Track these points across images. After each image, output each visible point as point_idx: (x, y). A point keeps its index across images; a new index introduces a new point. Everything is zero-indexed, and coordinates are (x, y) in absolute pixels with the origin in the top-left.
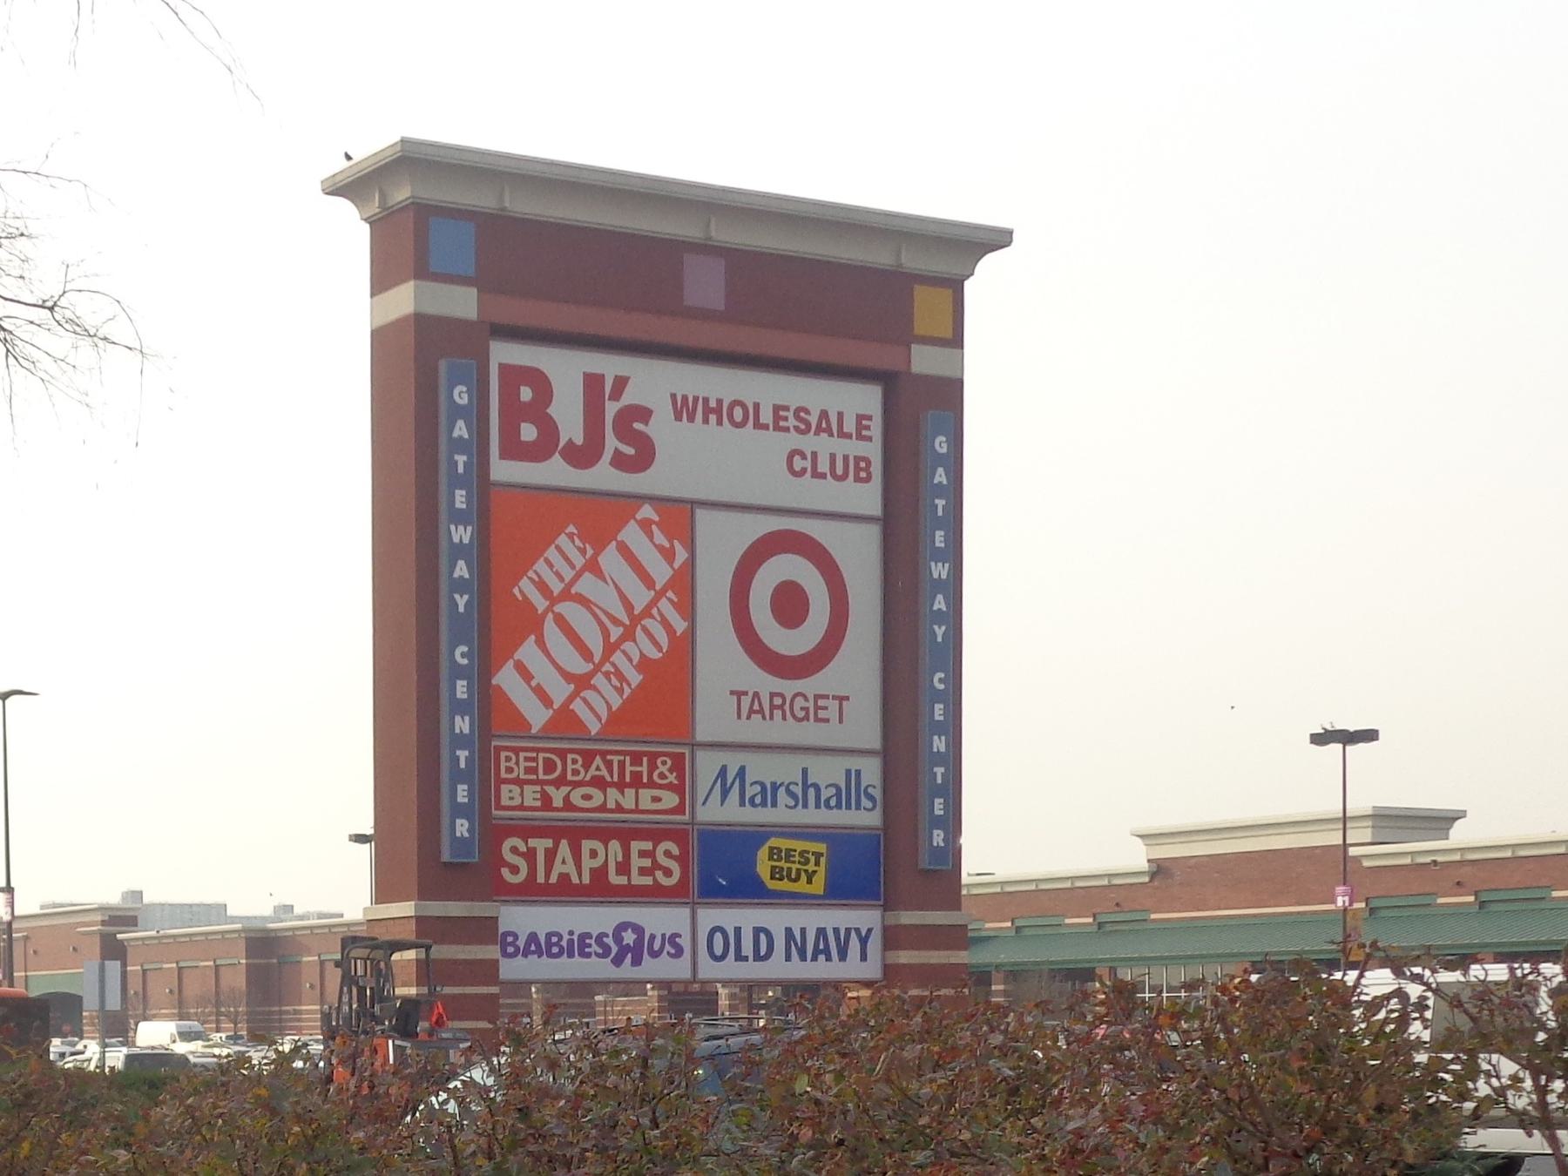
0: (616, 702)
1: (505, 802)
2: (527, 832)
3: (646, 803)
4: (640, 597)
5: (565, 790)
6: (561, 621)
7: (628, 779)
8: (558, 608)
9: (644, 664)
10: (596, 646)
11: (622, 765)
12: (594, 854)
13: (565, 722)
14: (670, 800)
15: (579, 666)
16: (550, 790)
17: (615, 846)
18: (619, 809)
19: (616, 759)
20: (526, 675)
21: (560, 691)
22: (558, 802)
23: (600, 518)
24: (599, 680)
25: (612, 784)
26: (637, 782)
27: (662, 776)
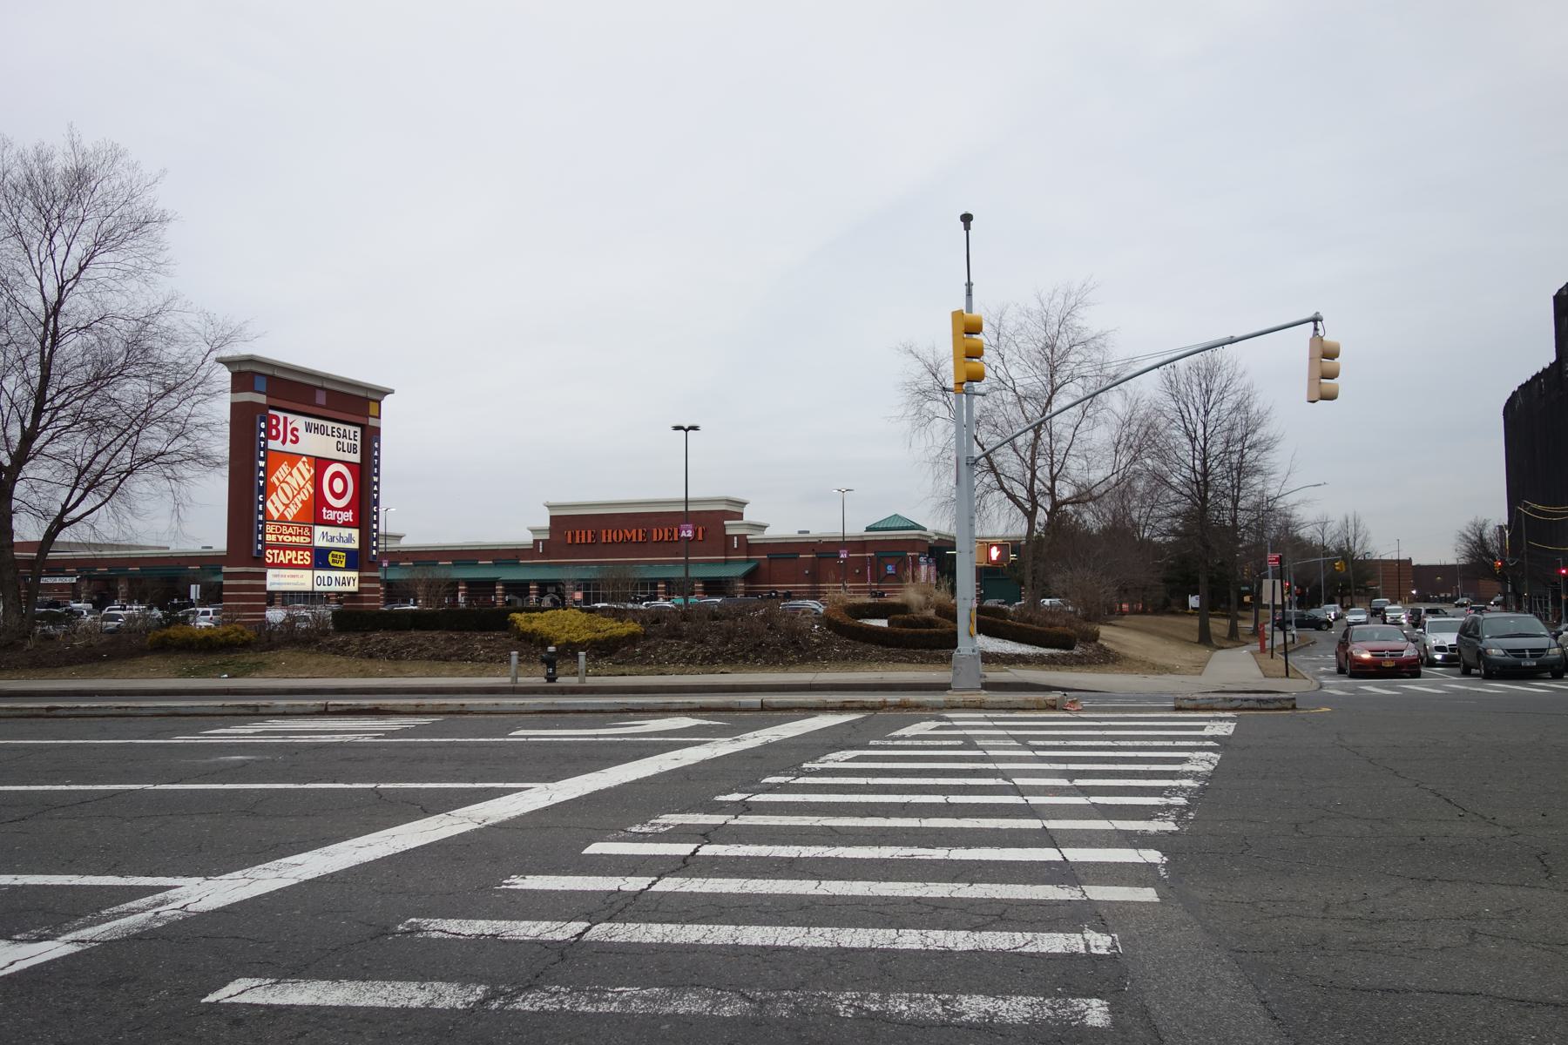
2: (273, 547)
4: (302, 483)
23: (293, 459)
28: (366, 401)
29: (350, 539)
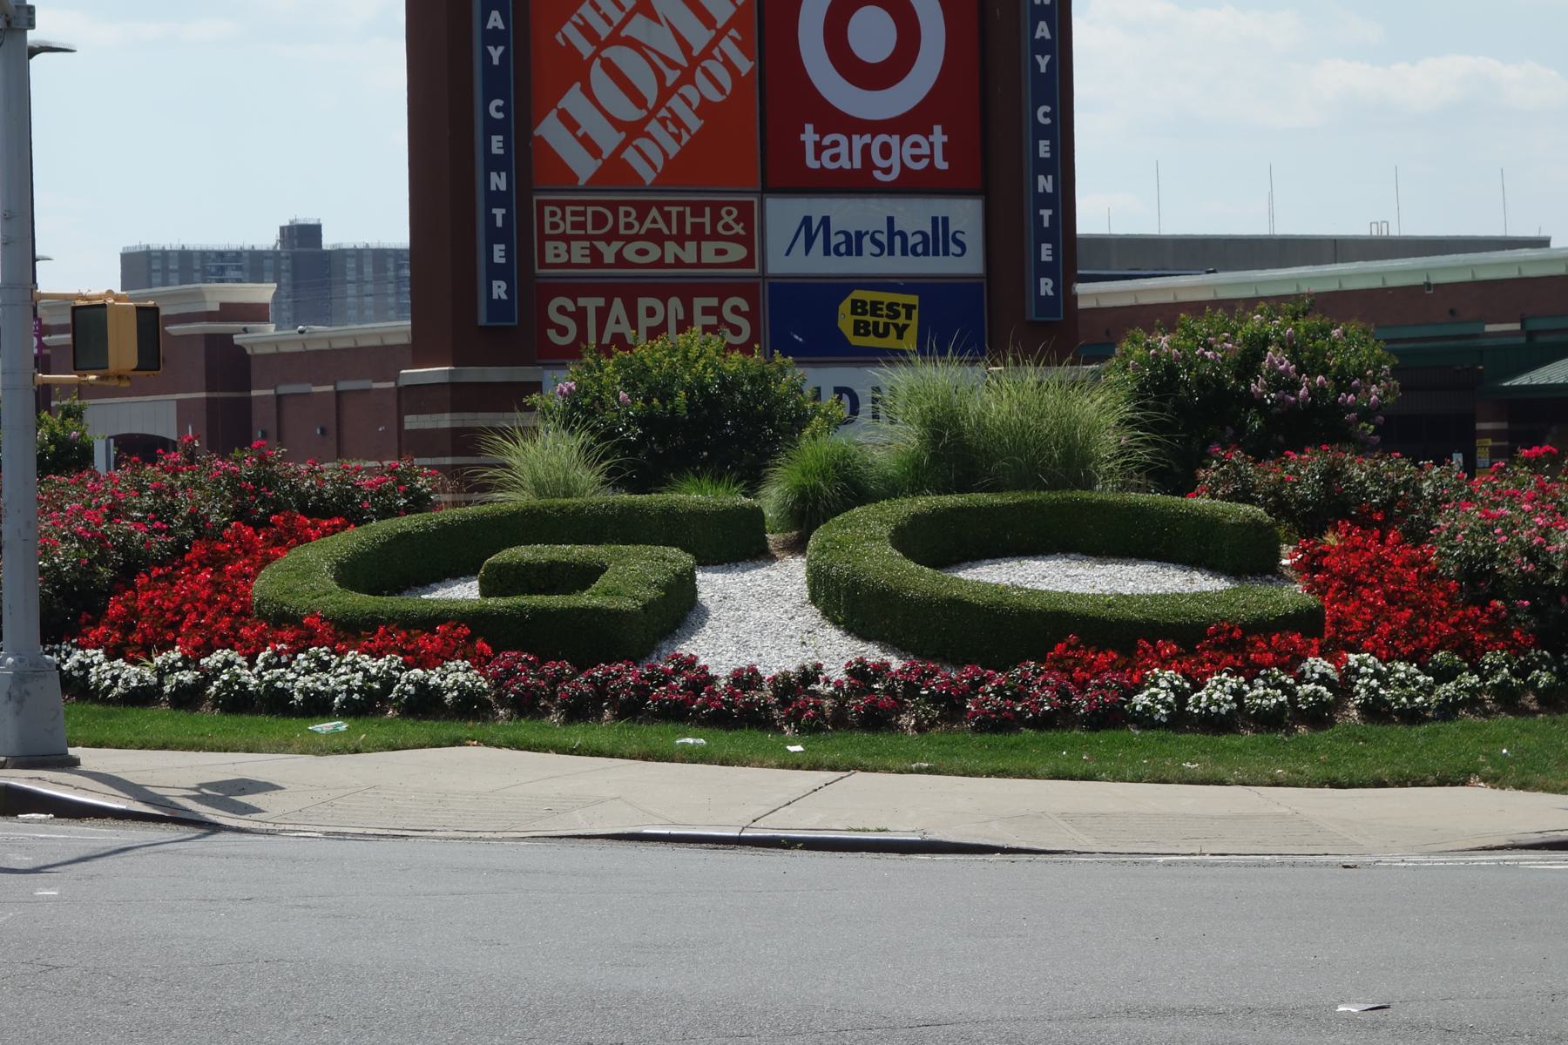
0: (673, 149)
1: (550, 259)
2: (575, 290)
3: (709, 256)
4: (700, 38)
5: (616, 245)
6: (611, 69)
7: (688, 231)
8: (605, 53)
9: (705, 109)
10: (651, 95)
11: (681, 216)
12: (651, 312)
13: (614, 172)
14: (737, 252)
15: (630, 113)
16: (601, 245)
17: (675, 303)
18: (679, 263)
19: (674, 210)
20: (570, 123)
21: (608, 140)
22: (609, 258)
24: (653, 127)
25: (670, 238)
26: (698, 235)
27: (727, 227)
29: (939, 238)
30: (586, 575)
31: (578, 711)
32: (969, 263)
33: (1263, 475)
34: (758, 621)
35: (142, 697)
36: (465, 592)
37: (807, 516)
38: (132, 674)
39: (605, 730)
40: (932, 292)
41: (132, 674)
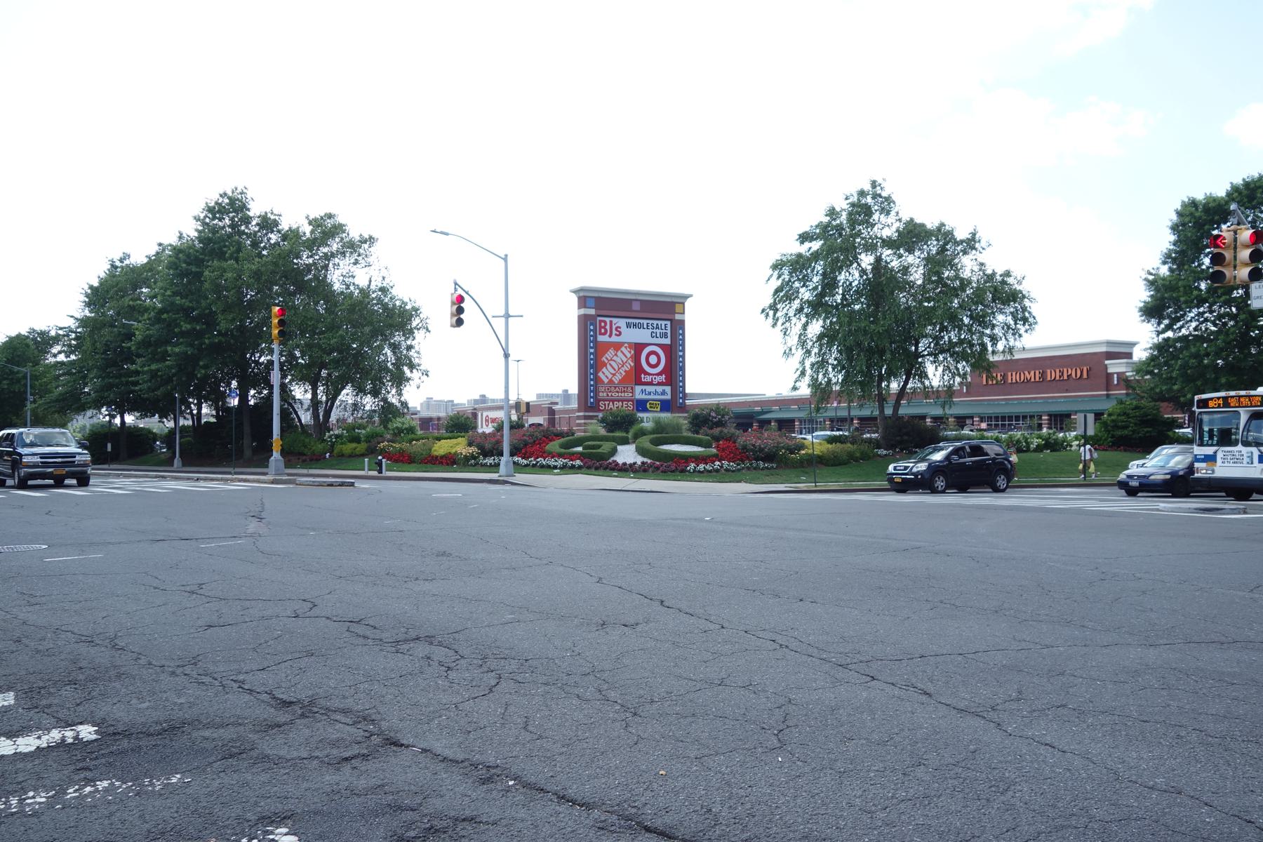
13: (611, 381)
23: (617, 346)
28: (673, 304)
29: (664, 393)
30: (599, 447)
31: (597, 469)
32: (668, 397)
33: (710, 432)
34: (627, 454)
35: (527, 465)
36: (580, 449)
37: (636, 437)
38: (525, 462)
39: (601, 472)
40: (662, 401)
41: (525, 462)
